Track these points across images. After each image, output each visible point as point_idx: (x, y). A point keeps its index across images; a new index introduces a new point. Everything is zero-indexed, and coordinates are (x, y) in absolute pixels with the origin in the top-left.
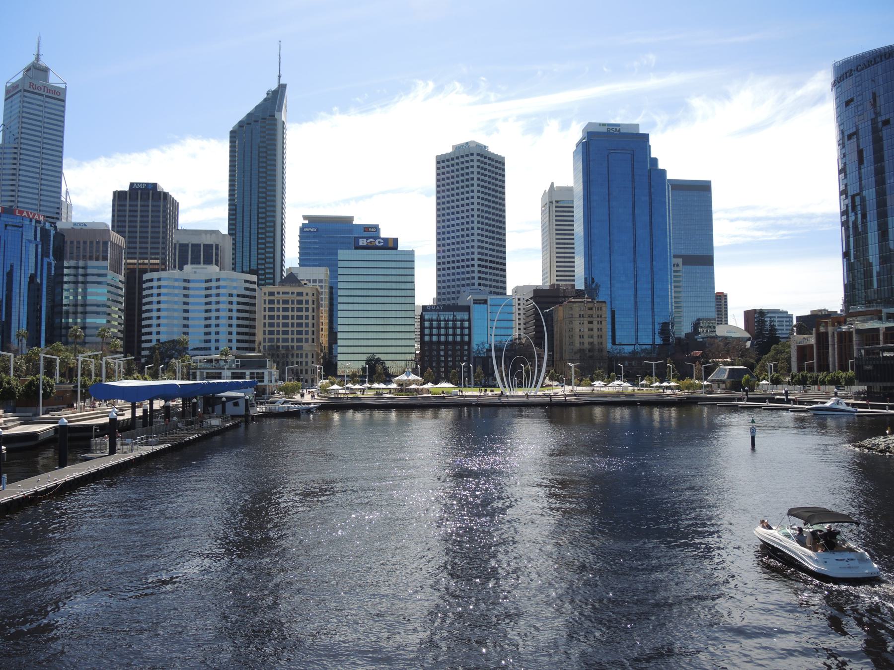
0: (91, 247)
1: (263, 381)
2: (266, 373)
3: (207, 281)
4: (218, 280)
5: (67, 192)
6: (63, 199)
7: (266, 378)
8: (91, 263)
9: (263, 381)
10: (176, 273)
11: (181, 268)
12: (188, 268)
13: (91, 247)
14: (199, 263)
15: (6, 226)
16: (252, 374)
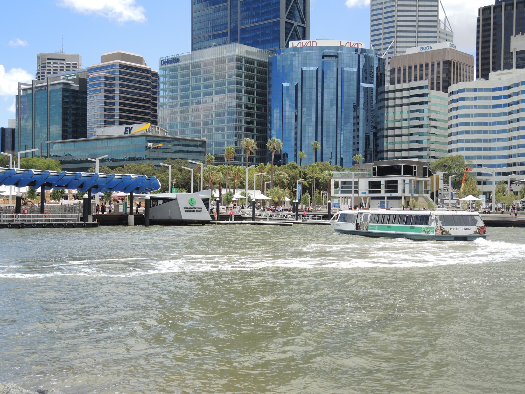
0: (433, 71)
1: (396, 192)
2: (400, 182)
3: (510, 87)
4: (518, 85)
5: (446, 18)
6: (442, 27)
7: (400, 188)
8: (414, 84)
9: (396, 192)
10: (482, 83)
11: (485, 76)
12: (492, 75)
13: (433, 71)
14: (511, 67)
15: (323, 57)
16: (387, 182)
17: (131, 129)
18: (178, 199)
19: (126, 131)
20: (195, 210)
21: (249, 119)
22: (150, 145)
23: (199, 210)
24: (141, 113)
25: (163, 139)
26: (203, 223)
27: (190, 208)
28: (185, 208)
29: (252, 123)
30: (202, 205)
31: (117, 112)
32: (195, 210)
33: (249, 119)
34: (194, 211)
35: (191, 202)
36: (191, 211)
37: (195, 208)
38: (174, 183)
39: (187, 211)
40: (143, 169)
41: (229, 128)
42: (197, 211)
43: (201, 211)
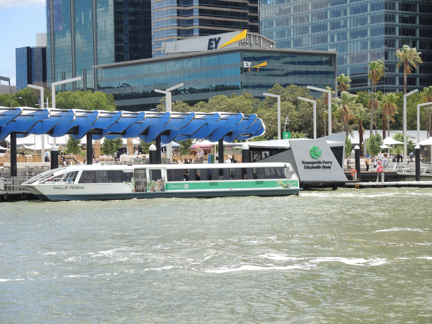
17: (217, 41)
18: (293, 149)
19: (210, 44)
20: (321, 165)
21: (407, 14)
22: (247, 64)
23: (327, 166)
24: (232, 15)
25: (268, 55)
26: (334, 186)
27: (313, 163)
28: (303, 162)
29: (412, 20)
30: (332, 158)
31: (196, 16)
32: (321, 165)
33: (407, 14)
34: (319, 167)
35: (314, 152)
36: (313, 167)
37: (320, 162)
38: (286, 123)
39: (308, 167)
40: (238, 104)
41: (374, 32)
42: (324, 167)
43: (329, 167)
